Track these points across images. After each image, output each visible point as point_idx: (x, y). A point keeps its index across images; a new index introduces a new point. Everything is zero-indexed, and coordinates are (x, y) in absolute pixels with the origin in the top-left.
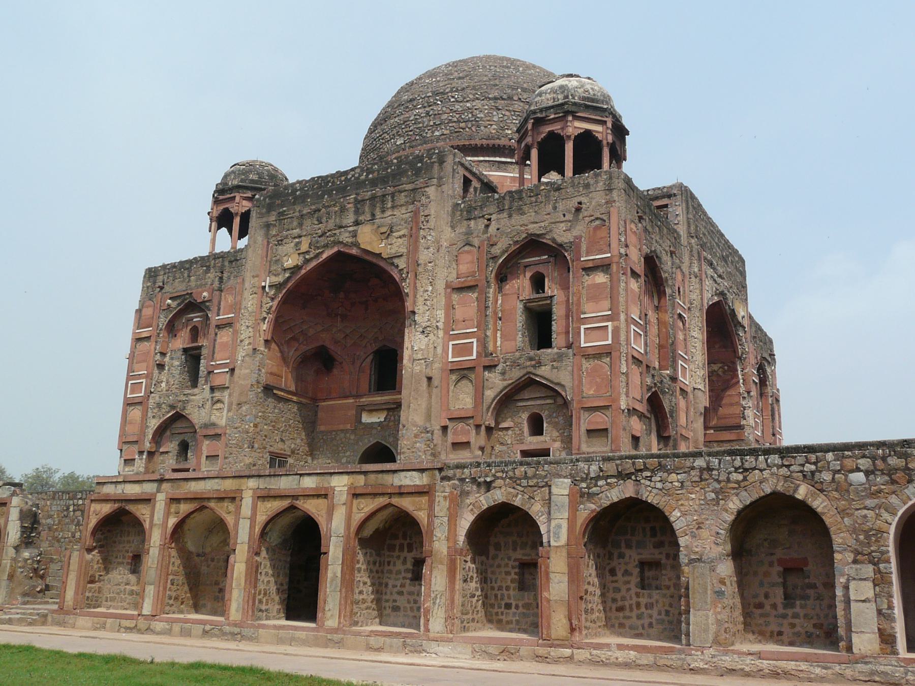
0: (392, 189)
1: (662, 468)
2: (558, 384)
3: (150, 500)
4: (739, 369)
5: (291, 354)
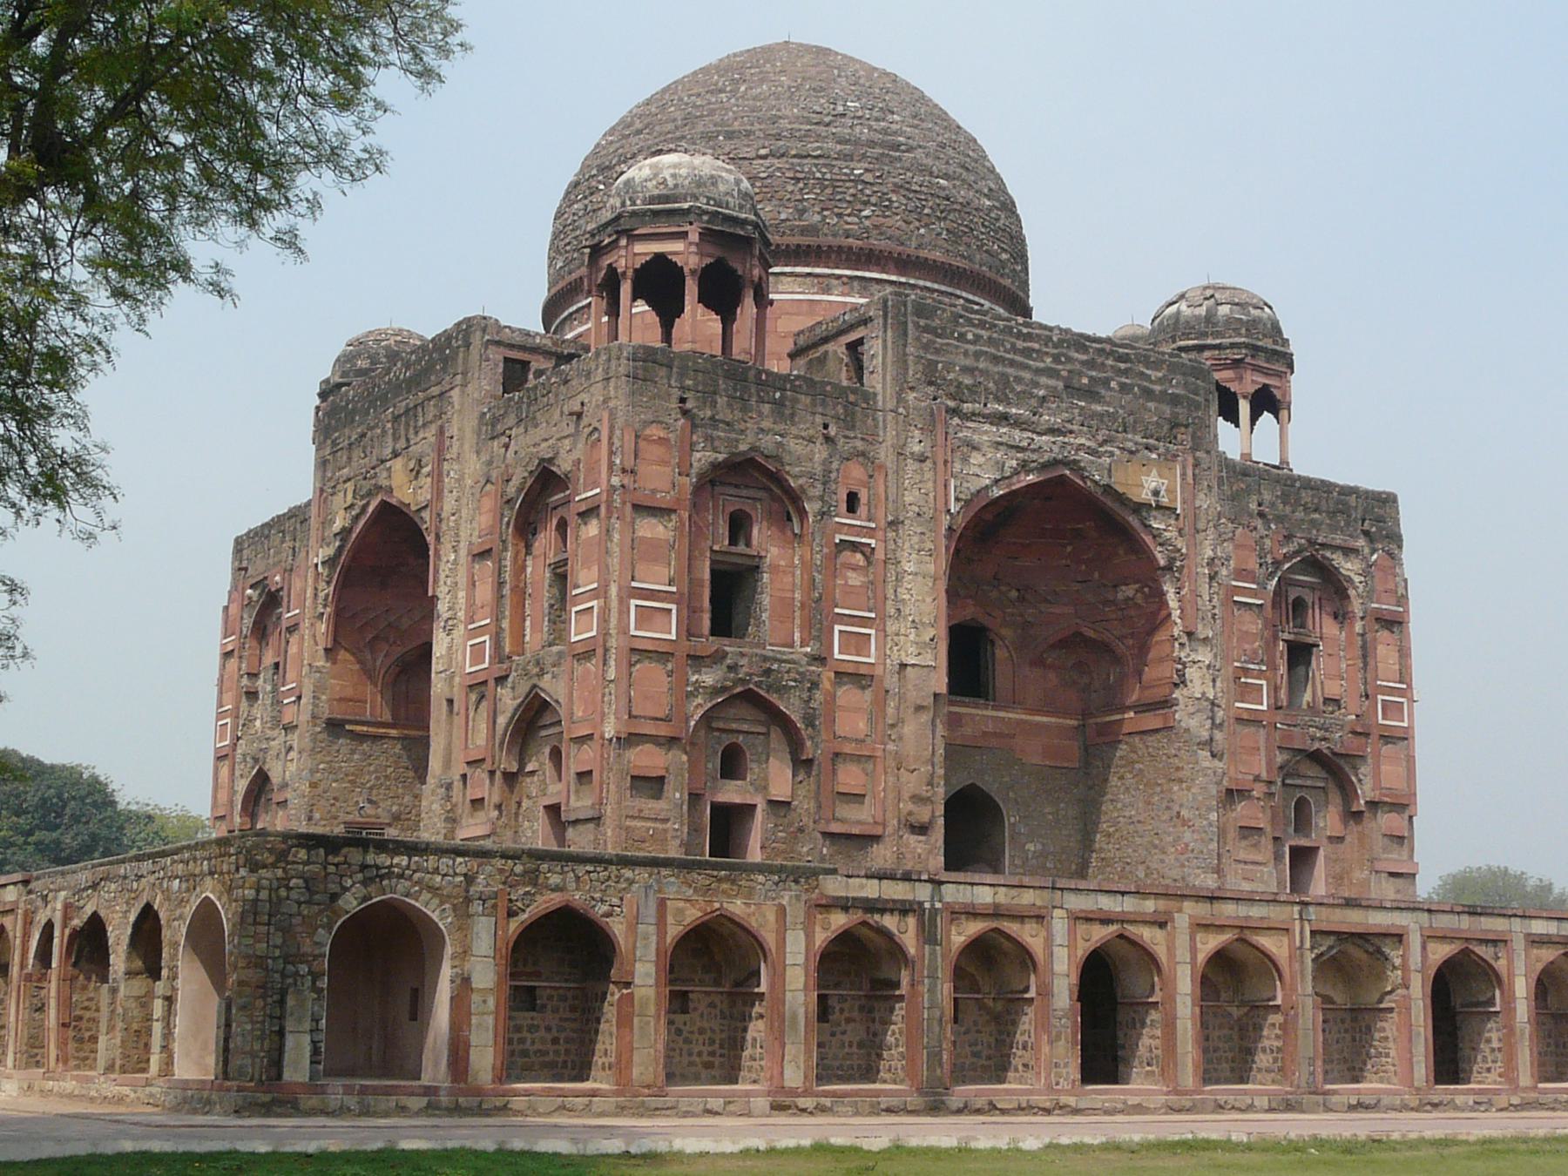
5: (378, 663)
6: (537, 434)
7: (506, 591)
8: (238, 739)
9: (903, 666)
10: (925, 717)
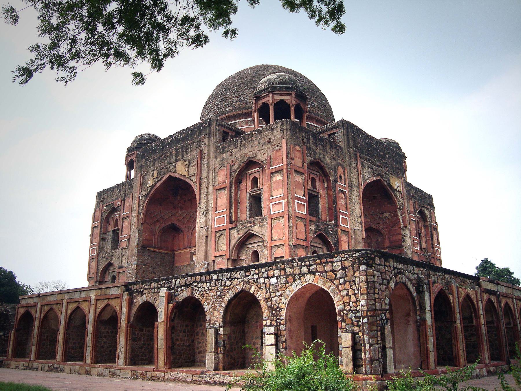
0: (190, 142)
1: (201, 281)
2: (262, 235)
3: (35, 306)
4: (399, 214)
6: (244, 151)
7: (233, 200)
8: (99, 253)
9: (354, 229)
10: (361, 245)
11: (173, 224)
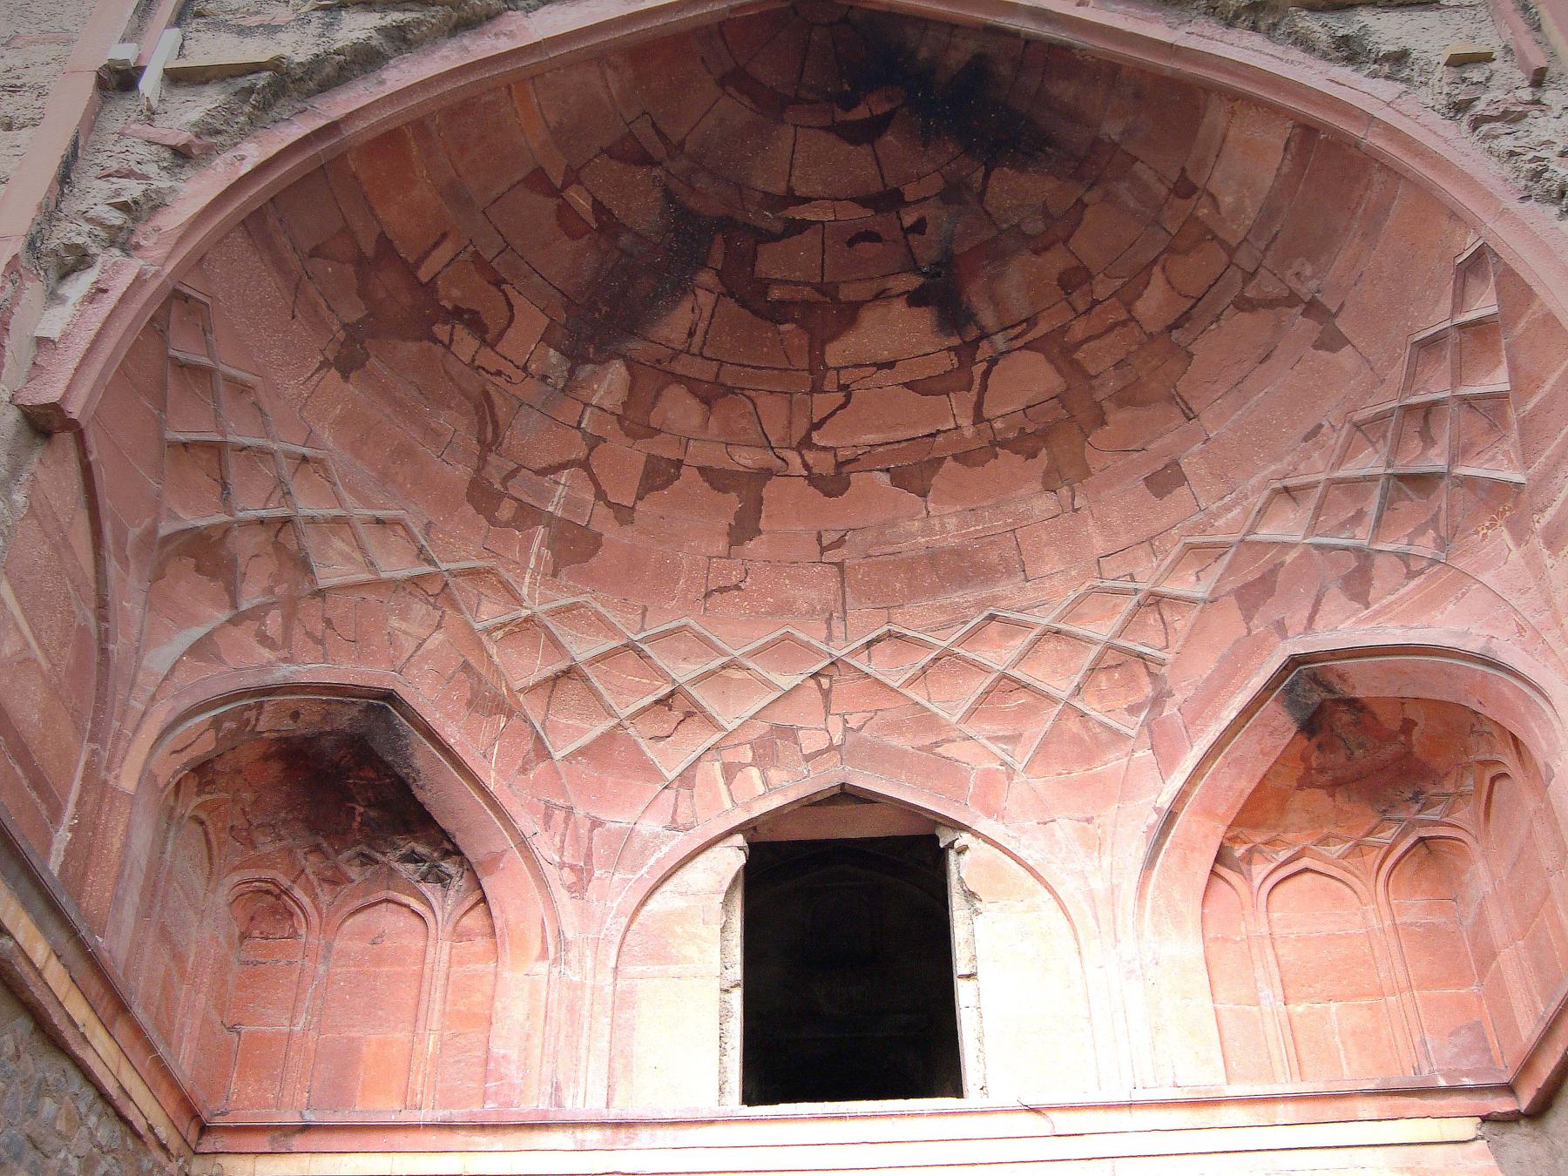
5: (161, 657)
11: (384, 703)
